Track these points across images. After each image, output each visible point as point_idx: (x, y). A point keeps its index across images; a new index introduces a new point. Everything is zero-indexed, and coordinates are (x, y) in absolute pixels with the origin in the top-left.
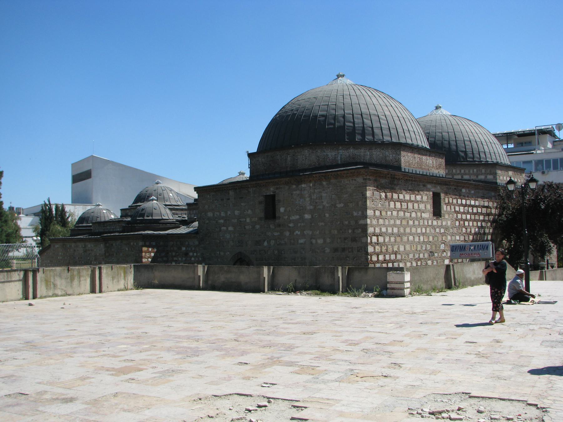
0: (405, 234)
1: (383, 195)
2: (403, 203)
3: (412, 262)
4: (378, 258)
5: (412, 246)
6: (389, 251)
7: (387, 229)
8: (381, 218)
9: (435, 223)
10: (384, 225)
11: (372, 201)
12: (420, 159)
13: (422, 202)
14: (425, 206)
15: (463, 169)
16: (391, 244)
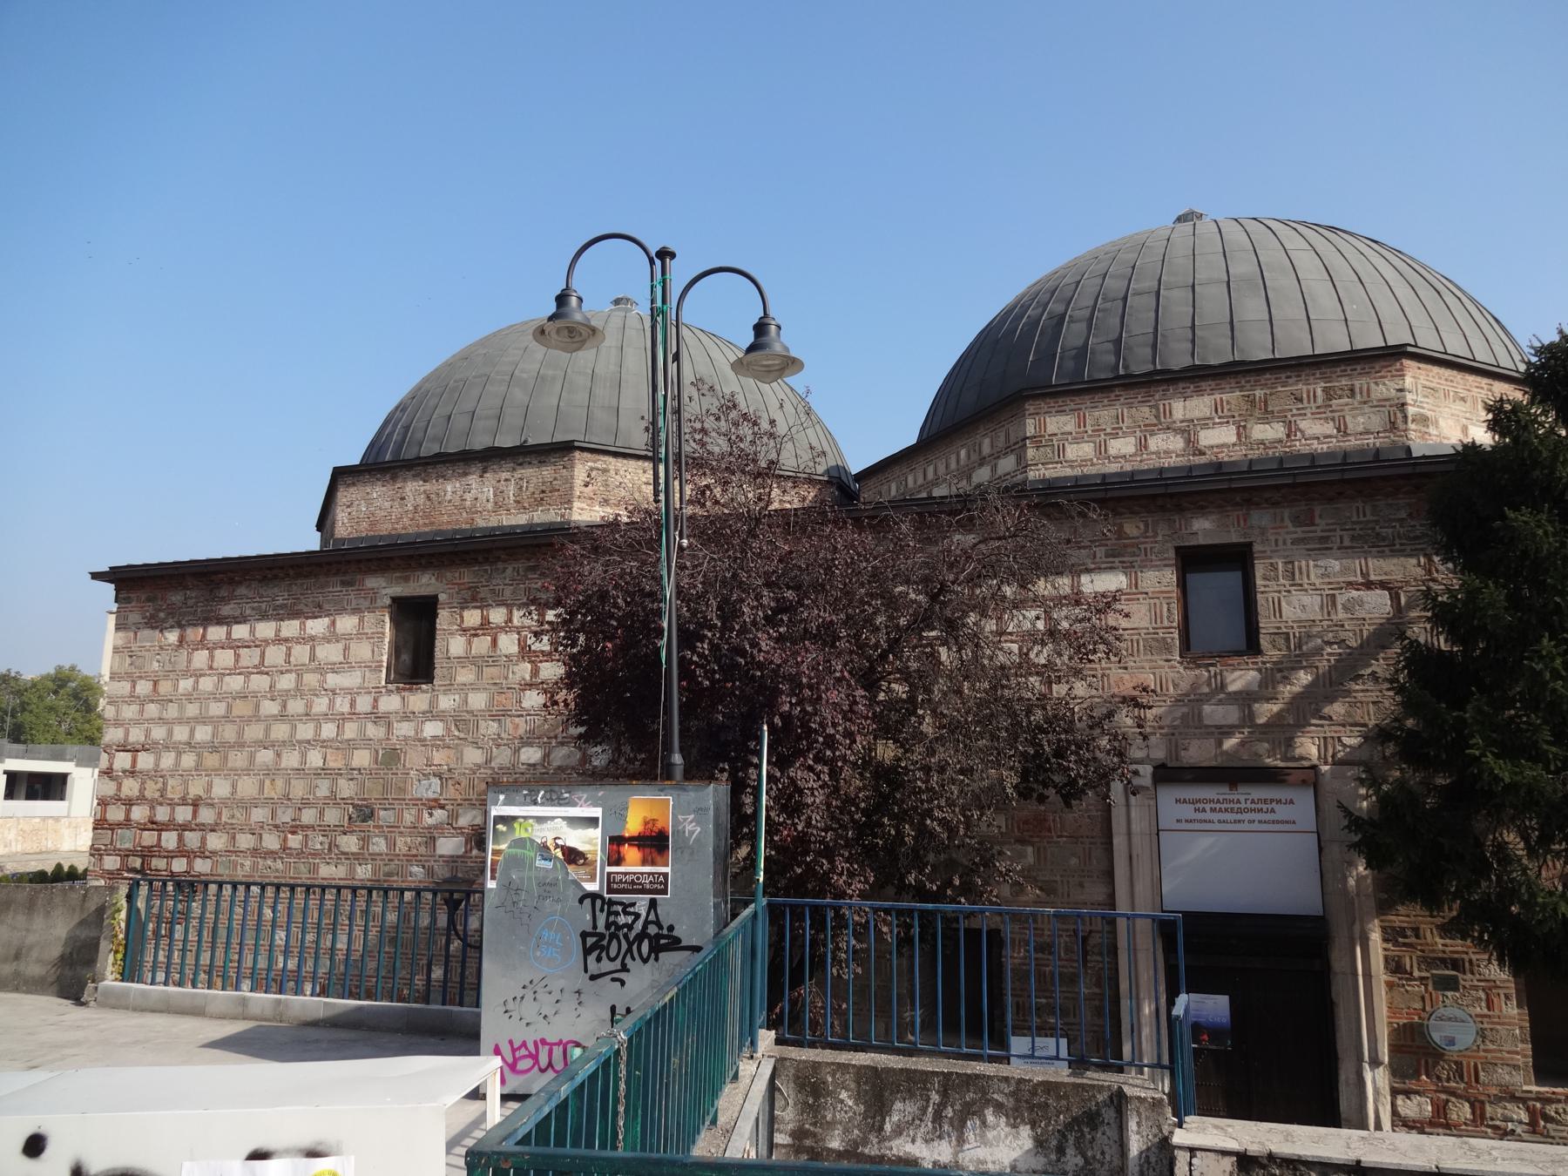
0: (240, 745)
1: (172, 637)
2: (243, 651)
3: (261, 834)
4: (128, 812)
5: (267, 782)
6: (170, 795)
7: (170, 733)
8: (152, 701)
9: (390, 703)
10: (161, 720)
11: (131, 656)
12: (428, 498)
13: (332, 636)
14: (346, 649)
15: (929, 463)
16: (182, 775)
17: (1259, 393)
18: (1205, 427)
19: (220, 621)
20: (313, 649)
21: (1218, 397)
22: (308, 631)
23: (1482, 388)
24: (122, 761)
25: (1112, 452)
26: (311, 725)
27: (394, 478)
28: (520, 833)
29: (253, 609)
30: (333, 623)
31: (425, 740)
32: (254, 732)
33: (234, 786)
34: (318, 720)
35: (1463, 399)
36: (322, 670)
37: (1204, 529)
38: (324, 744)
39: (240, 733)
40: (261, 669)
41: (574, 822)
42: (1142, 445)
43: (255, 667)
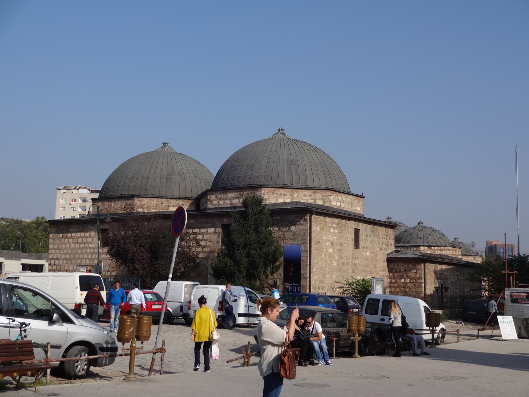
0: (74, 259)
1: (61, 235)
2: (74, 239)
6: (62, 269)
7: (61, 256)
8: (58, 249)
10: (60, 254)
12: (109, 206)
13: (90, 237)
14: (93, 239)
17: (242, 193)
18: (233, 199)
19: (70, 232)
20: (87, 239)
21: (236, 193)
22: (86, 235)
23: (283, 191)
24: (53, 262)
25: (220, 203)
26: (87, 255)
27: (102, 201)
28: (79, 270)
29: (76, 230)
30: (90, 234)
31: (106, 258)
32: (77, 256)
33: (73, 267)
34: (88, 254)
35: (278, 194)
36: (88, 244)
37: (225, 221)
38: (89, 259)
39: (74, 256)
40: (77, 243)
41: (84, 269)
42: (225, 202)
43: (76, 243)
